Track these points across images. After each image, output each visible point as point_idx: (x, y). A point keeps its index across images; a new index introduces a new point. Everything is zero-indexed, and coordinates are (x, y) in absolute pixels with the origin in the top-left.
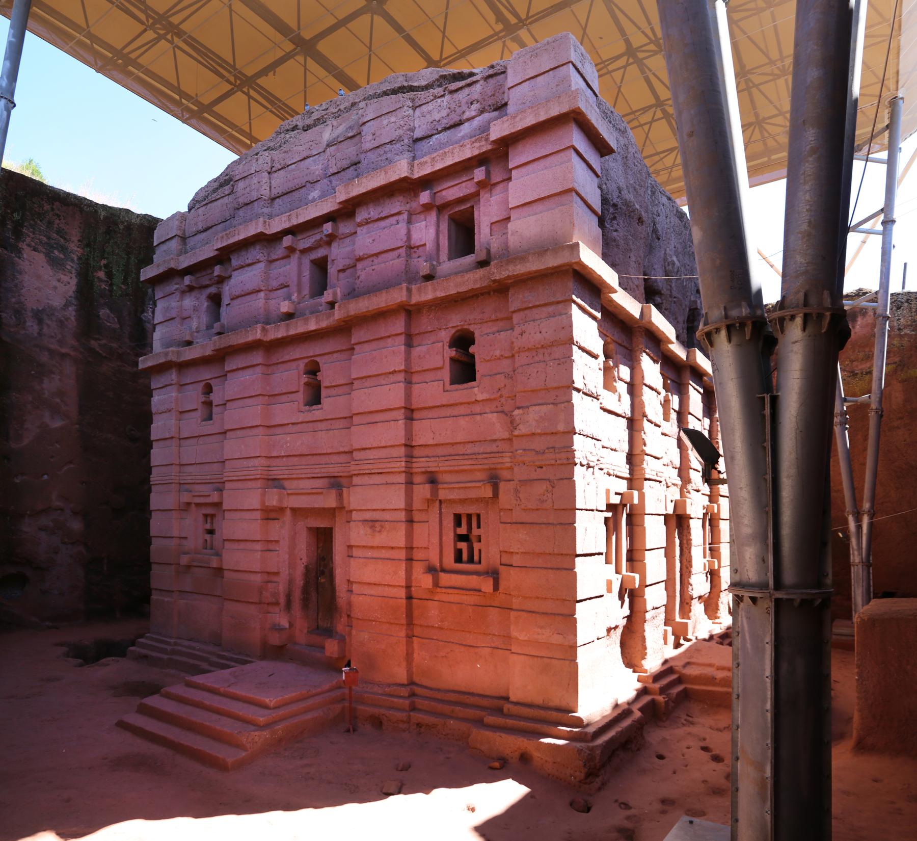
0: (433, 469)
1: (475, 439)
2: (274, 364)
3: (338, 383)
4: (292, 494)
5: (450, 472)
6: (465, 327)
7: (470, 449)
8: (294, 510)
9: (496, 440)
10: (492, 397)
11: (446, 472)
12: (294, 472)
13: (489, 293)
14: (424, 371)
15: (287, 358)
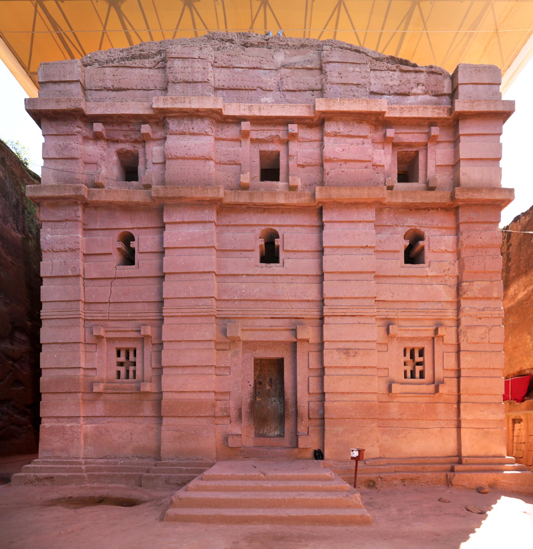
0: (393, 317)
1: (426, 300)
2: (224, 225)
3: (300, 249)
4: (246, 330)
5: (405, 320)
6: (418, 228)
7: (421, 306)
8: (245, 343)
9: (440, 302)
10: (440, 275)
11: (402, 319)
12: (249, 313)
13: (437, 209)
14: (384, 251)
15: (242, 222)
